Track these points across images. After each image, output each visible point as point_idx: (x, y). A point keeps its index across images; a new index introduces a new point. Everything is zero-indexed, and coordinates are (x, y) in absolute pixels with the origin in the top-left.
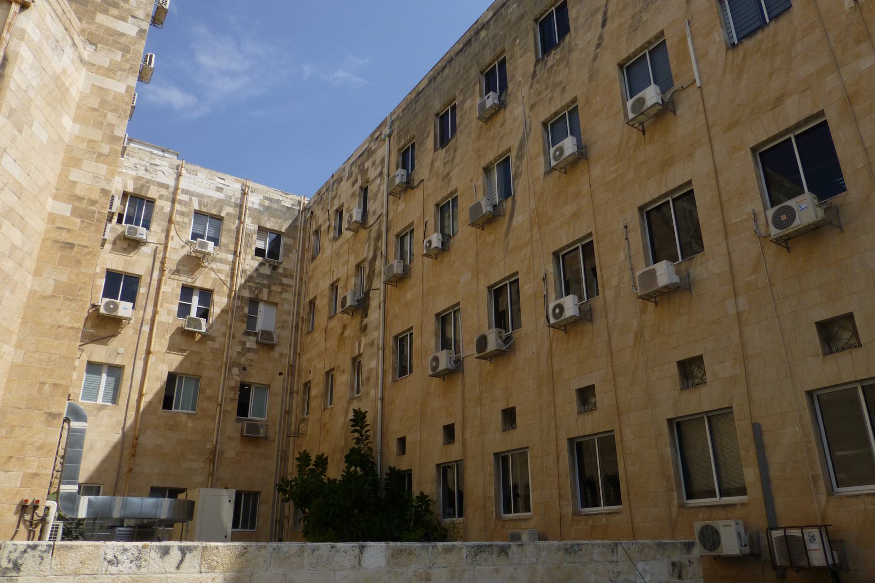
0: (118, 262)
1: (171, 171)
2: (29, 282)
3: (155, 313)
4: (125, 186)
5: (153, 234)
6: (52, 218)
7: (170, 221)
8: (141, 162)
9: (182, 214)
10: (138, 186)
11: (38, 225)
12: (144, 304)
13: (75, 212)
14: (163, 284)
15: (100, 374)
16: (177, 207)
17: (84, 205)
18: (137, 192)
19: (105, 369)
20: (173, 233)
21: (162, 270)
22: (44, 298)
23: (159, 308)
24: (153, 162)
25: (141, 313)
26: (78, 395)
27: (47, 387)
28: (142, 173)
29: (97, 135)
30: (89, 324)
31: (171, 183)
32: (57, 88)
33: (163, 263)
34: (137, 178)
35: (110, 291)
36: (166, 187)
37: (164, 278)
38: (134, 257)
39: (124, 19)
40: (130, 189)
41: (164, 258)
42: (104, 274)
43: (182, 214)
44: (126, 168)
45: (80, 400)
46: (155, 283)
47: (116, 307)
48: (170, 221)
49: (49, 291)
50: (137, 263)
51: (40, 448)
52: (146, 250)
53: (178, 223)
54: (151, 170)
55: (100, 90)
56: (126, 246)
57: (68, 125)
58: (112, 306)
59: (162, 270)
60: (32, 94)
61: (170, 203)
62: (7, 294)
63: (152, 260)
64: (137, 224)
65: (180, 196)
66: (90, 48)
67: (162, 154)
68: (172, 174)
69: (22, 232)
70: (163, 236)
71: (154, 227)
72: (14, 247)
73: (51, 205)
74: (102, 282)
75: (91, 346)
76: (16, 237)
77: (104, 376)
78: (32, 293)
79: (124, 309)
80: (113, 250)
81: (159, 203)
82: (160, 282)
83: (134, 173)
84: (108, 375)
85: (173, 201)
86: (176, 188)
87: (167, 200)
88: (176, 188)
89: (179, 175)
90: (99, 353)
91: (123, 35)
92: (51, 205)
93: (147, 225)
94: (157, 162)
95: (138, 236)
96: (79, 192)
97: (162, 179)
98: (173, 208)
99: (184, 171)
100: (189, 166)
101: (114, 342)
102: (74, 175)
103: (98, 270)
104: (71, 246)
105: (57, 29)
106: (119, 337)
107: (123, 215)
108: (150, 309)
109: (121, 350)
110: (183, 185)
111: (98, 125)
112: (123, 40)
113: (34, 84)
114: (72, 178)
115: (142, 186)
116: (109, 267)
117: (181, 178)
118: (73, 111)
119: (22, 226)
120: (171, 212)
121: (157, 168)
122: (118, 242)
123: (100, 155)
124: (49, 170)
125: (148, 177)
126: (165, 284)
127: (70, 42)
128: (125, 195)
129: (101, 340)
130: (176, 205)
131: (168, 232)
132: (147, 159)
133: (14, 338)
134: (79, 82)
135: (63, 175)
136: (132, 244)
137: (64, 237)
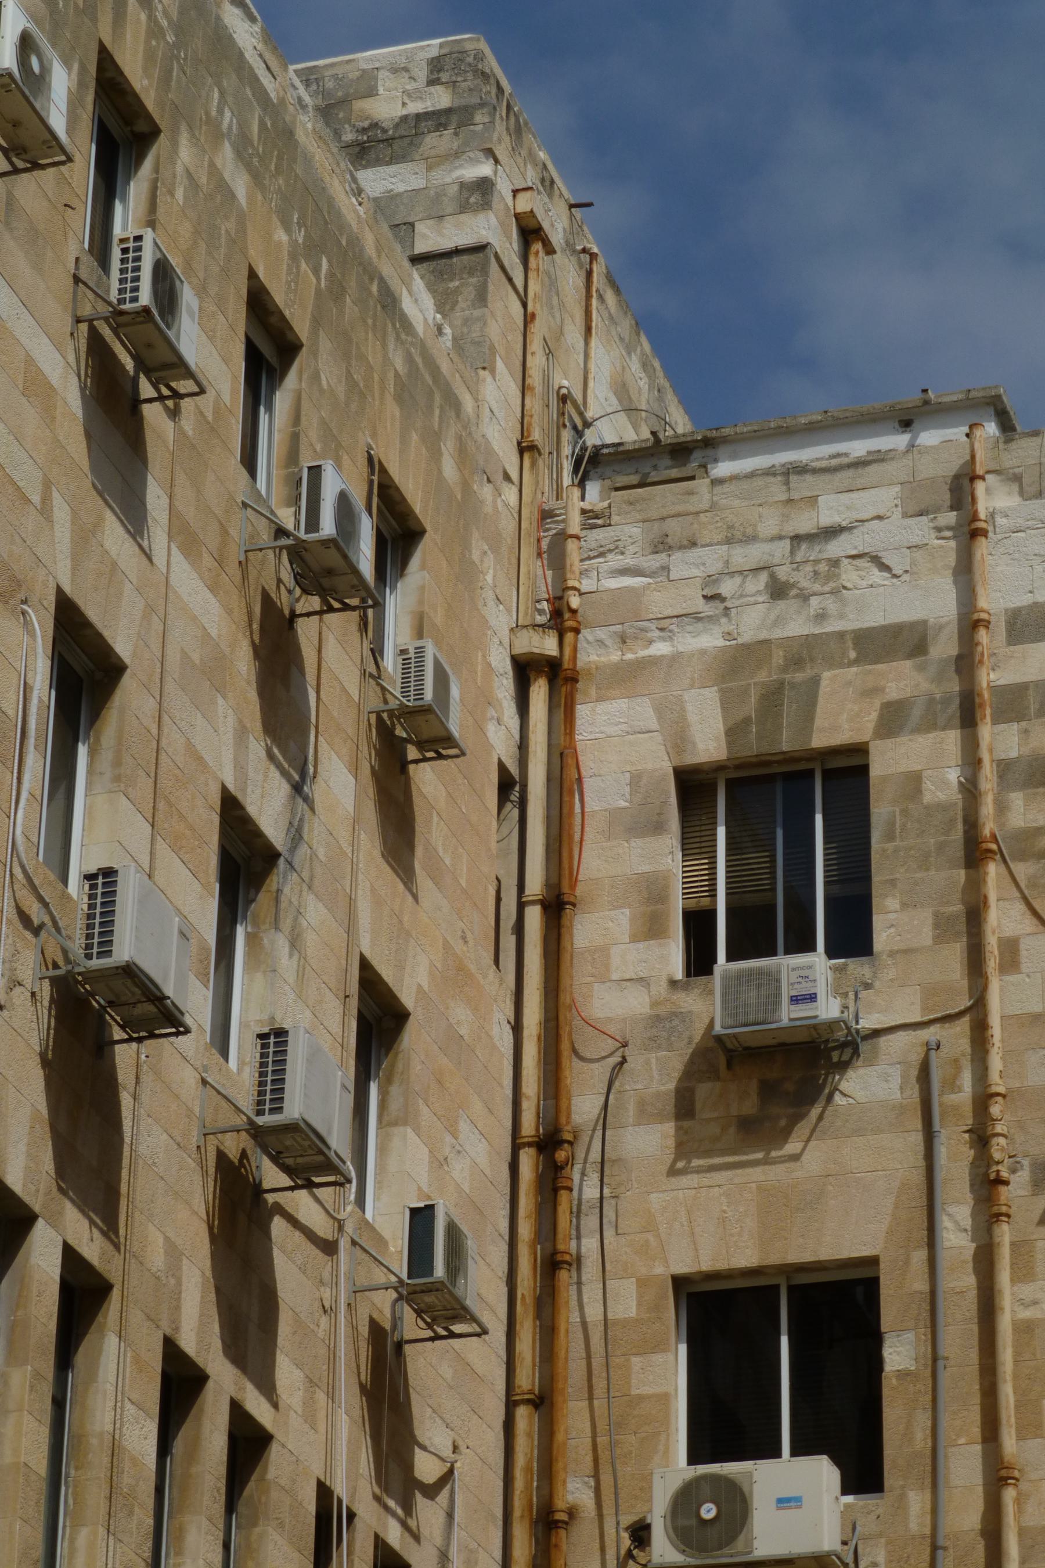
0: (720, 1219)
1: (921, 530)
3: (998, 1476)
4: (678, 736)
5: (890, 973)
7: (975, 853)
8: (744, 556)
10: (751, 707)
12: (921, 1438)
14: (1004, 1277)
16: (1001, 740)
18: (753, 746)
20: (1004, 918)
21: (987, 1185)
23: (1009, 1442)
24: (804, 523)
25: (917, 1502)
28: (754, 620)
31: (935, 603)
33: (981, 1137)
34: (736, 663)
35: (727, 1426)
36: (906, 641)
37: (1005, 1234)
38: (811, 1155)
40: (709, 746)
42: (669, 1316)
44: (665, 625)
46: (960, 1282)
47: (736, 1504)
50: (836, 1192)
52: (870, 1086)
53: (1027, 844)
54: (803, 579)
56: (750, 1106)
58: (708, 1511)
59: (987, 1185)
61: (952, 738)
63: (917, 1138)
64: (802, 943)
65: (1004, 668)
67: (899, 441)
68: (929, 536)
70: (955, 953)
71: (892, 923)
74: (667, 1376)
80: (685, 1150)
81: (887, 762)
82: (985, 1261)
83: (710, 640)
86: (971, 624)
87: (929, 724)
88: (971, 624)
89: (971, 532)
93: (852, 937)
94: (830, 510)
95: (788, 1014)
97: (878, 602)
98: (972, 761)
99: (993, 499)
100: (1025, 452)
103: (626, 1304)
107: (711, 914)
108: (965, 1466)
110: (996, 599)
115: (772, 698)
116: (682, 1268)
117: (982, 547)
120: (970, 790)
121: (836, 548)
122: (704, 1090)
125: (798, 627)
126: (1023, 1272)
128: (693, 787)
130: (986, 731)
131: (975, 916)
132: (769, 525)
136: (767, 1082)
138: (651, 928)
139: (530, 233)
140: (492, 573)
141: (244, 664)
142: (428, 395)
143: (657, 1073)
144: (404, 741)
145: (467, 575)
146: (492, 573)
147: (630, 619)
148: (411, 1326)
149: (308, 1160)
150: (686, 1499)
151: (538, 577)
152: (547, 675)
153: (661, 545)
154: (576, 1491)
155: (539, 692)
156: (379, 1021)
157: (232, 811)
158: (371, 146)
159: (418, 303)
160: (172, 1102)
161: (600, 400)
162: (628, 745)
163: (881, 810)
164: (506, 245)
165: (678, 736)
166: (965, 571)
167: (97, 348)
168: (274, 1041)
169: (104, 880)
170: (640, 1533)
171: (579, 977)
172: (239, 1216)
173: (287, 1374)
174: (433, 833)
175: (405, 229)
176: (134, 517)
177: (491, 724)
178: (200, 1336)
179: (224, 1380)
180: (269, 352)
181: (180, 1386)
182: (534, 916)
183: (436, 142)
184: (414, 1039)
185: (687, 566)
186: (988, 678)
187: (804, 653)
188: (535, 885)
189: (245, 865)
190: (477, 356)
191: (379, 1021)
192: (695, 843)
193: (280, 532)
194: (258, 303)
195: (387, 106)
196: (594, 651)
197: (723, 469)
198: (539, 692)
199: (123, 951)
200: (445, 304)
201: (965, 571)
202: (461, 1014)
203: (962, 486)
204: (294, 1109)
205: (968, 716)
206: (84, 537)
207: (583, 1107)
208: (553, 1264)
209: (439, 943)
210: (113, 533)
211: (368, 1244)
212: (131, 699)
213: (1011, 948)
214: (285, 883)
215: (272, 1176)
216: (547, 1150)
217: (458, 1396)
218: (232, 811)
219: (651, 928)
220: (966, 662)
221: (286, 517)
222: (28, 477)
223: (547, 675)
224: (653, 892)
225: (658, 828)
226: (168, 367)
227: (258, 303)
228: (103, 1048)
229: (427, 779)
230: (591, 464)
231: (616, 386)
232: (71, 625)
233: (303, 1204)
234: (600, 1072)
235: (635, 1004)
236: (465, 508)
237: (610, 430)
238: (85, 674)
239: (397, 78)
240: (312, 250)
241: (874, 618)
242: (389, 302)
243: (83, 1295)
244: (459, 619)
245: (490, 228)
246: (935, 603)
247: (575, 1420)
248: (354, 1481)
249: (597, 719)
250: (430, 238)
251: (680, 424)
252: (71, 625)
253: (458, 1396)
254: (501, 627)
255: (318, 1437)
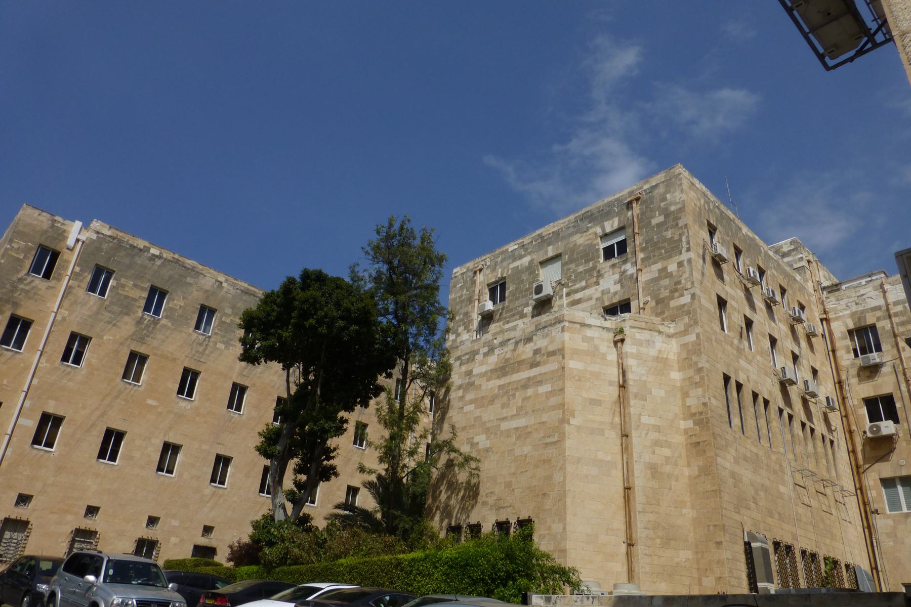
0: (869, 389)
1: (877, 293)
2: (686, 472)
4: (846, 326)
6: (686, 431)
7: (895, 336)
9: (903, 324)
11: (679, 439)
13: (695, 423)
15: (896, 487)
16: (895, 320)
17: (697, 417)
19: (898, 482)
22: (695, 478)
24: (859, 294)
26: (884, 509)
27: (711, 528)
28: (854, 308)
29: (691, 372)
30: (868, 449)
31: (881, 302)
32: (661, 361)
33: (905, 374)
34: (853, 315)
35: (874, 417)
36: (878, 308)
38: (879, 380)
39: (682, 295)
40: (851, 326)
41: (904, 369)
43: (903, 324)
44: (841, 311)
45: (888, 512)
47: (879, 428)
48: (895, 336)
49: (697, 473)
50: (884, 384)
51: (718, 563)
55: (684, 346)
57: (676, 376)
60: (644, 378)
61: (888, 321)
62: (673, 483)
64: (871, 352)
65: (894, 310)
66: (673, 325)
69: (669, 447)
70: (895, 351)
71: (884, 347)
72: (667, 458)
73: (684, 424)
74: (864, 411)
75: (877, 466)
76: (667, 452)
77: (900, 488)
78: (690, 476)
79: (887, 427)
80: (860, 381)
81: (879, 325)
83: (848, 312)
84: (902, 486)
85: (890, 317)
86: (887, 305)
87: (884, 319)
88: (887, 305)
89: (884, 292)
90: (886, 469)
91: (684, 305)
92: (684, 424)
93: (879, 349)
94: (862, 292)
95: (872, 362)
96: (693, 410)
97: (872, 303)
99: (887, 287)
101: (894, 457)
102: (689, 402)
103: (856, 402)
104: (699, 443)
105: (646, 335)
106: (896, 451)
109: (903, 462)
111: (690, 366)
112: (686, 308)
113: (643, 372)
114: (688, 404)
115: (859, 319)
118: (676, 366)
119: (668, 445)
120: (893, 327)
123: (696, 383)
124: (675, 407)
127: (657, 334)
128: (850, 332)
129: (884, 457)
131: (897, 344)
132: (853, 295)
133: (688, 504)
134: (672, 349)
135: (684, 404)
136: (871, 371)
137: (694, 440)
138: (849, 352)
139: (809, 262)
140: (814, 308)
141: (790, 333)
142: (802, 289)
143: (854, 371)
144: (809, 336)
145: (812, 310)
146: (814, 308)
147: (836, 311)
148: (828, 411)
149: (814, 395)
150: (871, 428)
151: (821, 307)
152: (825, 320)
153: (838, 300)
154: (854, 428)
155: (824, 323)
156: (815, 372)
157: (793, 352)
158: (784, 255)
159: (798, 278)
160: (794, 392)
161: (822, 280)
162: (839, 328)
163: (879, 332)
164: (806, 264)
165: (846, 326)
166: (885, 297)
167: (766, 302)
168: (806, 382)
169: (783, 369)
170: (865, 432)
171: (839, 360)
172: (805, 402)
173: (815, 421)
174: (816, 346)
175: (791, 266)
176: (774, 320)
177: (819, 330)
178: (804, 419)
179: (808, 424)
180: (783, 291)
181: (803, 425)
182: (831, 353)
183: (793, 253)
184: (819, 373)
185: (842, 302)
186: (892, 312)
187: (863, 312)
188: (830, 348)
189: (795, 358)
190: (806, 280)
191: (815, 372)
192: (852, 339)
193: (790, 316)
194: (781, 287)
195: (785, 249)
196: (831, 316)
197: (843, 287)
198: (824, 323)
199: (788, 377)
200: (800, 274)
201: (885, 297)
202: (824, 369)
203: (882, 286)
204: (811, 390)
205: (890, 317)
206: (770, 325)
207: (844, 377)
208: (844, 398)
209: (820, 360)
210: (773, 324)
211: (820, 402)
212: (779, 343)
213: (904, 349)
214: (800, 359)
215: (808, 397)
216: (840, 383)
217: (835, 419)
218: (793, 353)
219: (849, 352)
220: (888, 310)
221: (791, 312)
222: (762, 321)
223: (825, 320)
224: (847, 347)
225: (846, 338)
226: (775, 302)
227: (781, 287)
228: (786, 387)
229: (813, 340)
230: (823, 289)
231: (825, 277)
232: (770, 336)
233: (813, 400)
234: (845, 373)
235: (848, 362)
236: (810, 301)
237: (826, 283)
238: (773, 341)
239: (785, 245)
240: (784, 278)
241: (872, 306)
242: (795, 279)
243: (791, 417)
244: (813, 316)
245: (804, 263)
246: (881, 302)
247: (852, 419)
248: (825, 432)
249: (834, 325)
250: (795, 266)
251: (836, 281)
252: (770, 336)
253: (835, 419)
254: (817, 315)
255: (820, 427)
